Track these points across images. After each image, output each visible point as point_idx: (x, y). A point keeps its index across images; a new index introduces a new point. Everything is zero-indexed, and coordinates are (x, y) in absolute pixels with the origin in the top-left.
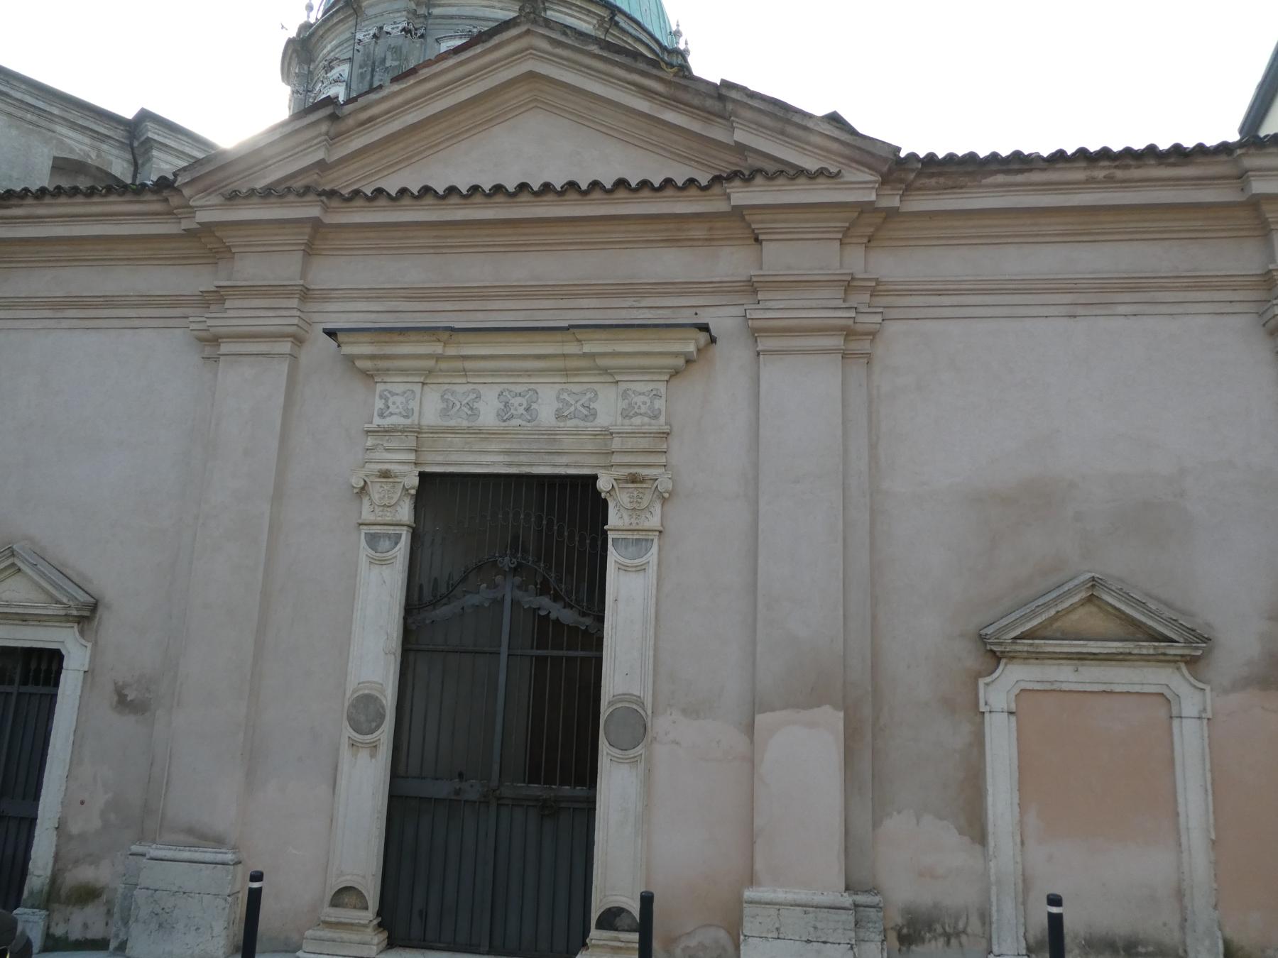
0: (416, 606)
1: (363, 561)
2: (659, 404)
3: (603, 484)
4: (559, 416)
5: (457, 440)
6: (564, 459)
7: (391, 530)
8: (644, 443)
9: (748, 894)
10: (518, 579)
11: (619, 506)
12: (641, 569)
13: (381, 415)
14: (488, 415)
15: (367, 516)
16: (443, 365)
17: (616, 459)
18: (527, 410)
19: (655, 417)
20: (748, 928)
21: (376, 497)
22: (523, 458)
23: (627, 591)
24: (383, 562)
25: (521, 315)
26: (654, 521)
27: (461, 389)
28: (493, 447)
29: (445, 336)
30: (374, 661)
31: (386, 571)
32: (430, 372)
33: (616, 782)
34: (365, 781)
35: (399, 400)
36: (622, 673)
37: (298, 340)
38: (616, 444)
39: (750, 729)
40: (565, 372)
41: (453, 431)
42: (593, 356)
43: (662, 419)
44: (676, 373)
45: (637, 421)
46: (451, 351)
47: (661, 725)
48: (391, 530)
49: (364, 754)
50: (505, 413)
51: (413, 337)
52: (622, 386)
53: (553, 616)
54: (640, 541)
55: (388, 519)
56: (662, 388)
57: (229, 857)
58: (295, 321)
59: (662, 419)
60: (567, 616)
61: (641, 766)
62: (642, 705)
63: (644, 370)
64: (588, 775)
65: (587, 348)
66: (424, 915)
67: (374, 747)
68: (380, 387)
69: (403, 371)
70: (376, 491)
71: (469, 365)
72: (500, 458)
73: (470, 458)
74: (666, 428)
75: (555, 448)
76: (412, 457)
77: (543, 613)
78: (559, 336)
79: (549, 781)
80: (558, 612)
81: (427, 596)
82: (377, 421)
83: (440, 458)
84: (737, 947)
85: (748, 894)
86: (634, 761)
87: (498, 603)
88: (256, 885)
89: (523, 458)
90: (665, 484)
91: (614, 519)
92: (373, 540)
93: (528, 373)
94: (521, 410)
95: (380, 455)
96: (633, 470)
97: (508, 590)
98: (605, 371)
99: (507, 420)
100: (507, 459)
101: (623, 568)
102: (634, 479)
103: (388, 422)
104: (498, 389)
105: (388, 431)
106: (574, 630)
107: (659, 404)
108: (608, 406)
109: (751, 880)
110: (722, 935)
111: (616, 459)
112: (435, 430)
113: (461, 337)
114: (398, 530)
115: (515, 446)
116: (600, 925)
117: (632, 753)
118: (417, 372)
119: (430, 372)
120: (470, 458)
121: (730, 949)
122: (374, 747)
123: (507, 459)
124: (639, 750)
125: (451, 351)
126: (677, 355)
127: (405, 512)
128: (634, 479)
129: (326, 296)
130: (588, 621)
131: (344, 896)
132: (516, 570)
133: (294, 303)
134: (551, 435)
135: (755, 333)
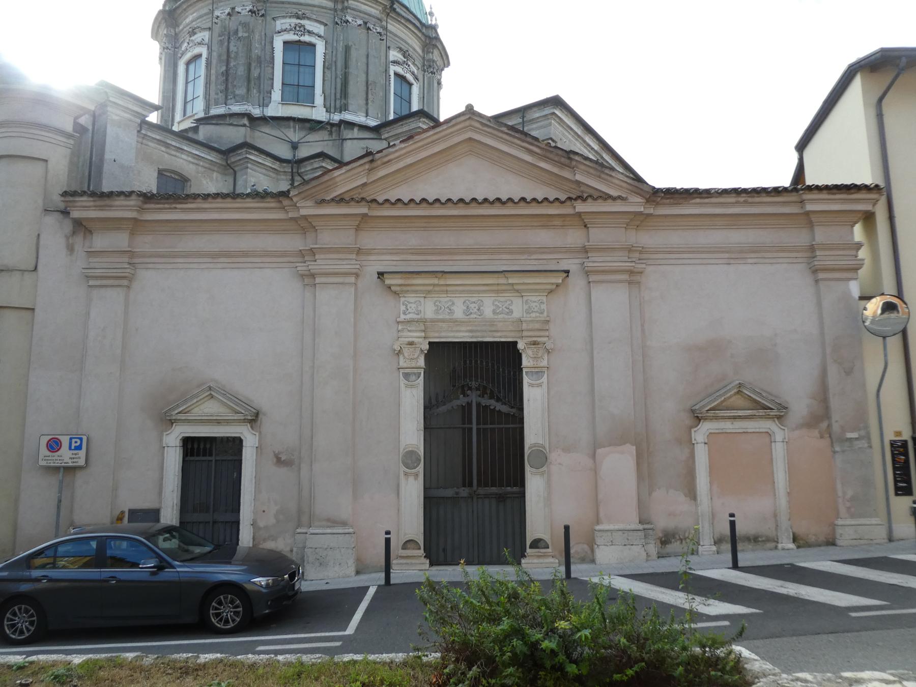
0: (428, 407)
1: (402, 385)
2: (544, 307)
3: (520, 346)
4: (494, 312)
5: (444, 325)
6: (499, 334)
7: (415, 371)
8: (537, 326)
9: (597, 528)
10: (478, 392)
11: (528, 356)
12: (540, 385)
13: (404, 313)
14: (459, 312)
15: (402, 364)
16: (437, 289)
17: (525, 333)
18: (478, 310)
19: (542, 313)
20: (599, 541)
21: (406, 354)
22: (479, 334)
23: (534, 396)
24: (412, 386)
25: (472, 263)
26: (544, 363)
27: (444, 300)
28: (463, 329)
29: (440, 275)
30: (411, 433)
31: (414, 391)
32: (429, 292)
33: (534, 484)
34: (413, 491)
35: (413, 306)
36: (534, 433)
37: (357, 275)
38: (524, 326)
39: (593, 456)
40: (497, 292)
41: (443, 321)
42: (513, 284)
43: (545, 314)
44: (551, 292)
45: (533, 315)
46: (442, 282)
47: (553, 456)
48: (415, 371)
49: (411, 479)
50: (467, 312)
51: (423, 275)
52: (525, 298)
53: (497, 409)
54: (538, 372)
55: (413, 365)
56: (544, 299)
57: (351, 530)
58: (358, 266)
59: (545, 314)
60: (504, 409)
61: (546, 476)
62: (544, 448)
63: (536, 291)
64: (521, 482)
65: (510, 281)
66: (444, 550)
67: (416, 475)
68: (402, 299)
69: (416, 292)
70: (406, 352)
71: (449, 288)
72: (467, 334)
73: (452, 334)
74: (548, 319)
75: (493, 329)
76: (423, 334)
77: (492, 407)
78: (496, 275)
79: (501, 485)
80: (499, 407)
81: (434, 402)
82: (402, 317)
83: (437, 335)
84: (593, 551)
85: (597, 528)
86: (542, 474)
87: (469, 405)
88: (388, 536)
89: (479, 334)
90: (549, 345)
91: (525, 362)
92: (407, 376)
93: (479, 292)
94: (475, 310)
95: (406, 334)
96: (535, 339)
97: (474, 397)
98: (517, 291)
99: (473, 315)
100: (471, 334)
101: (531, 385)
102: (535, 343)
103: (409, 317)
104: (462, 300)
105: (409, 322)
106: (507, 415)
107: (544, 307)
108: (518, 308)
109: (598, 522)
110: (585, 546)
111: (525, 333)
112: (433, 321)
113: (448, 276)
114: (419, 371)
115: (474, 328)
116: (531, 547)
117: (541, 470)
118: (421, 292)
119: (429, 292)
120: (452, 334)
121: (589, 552)
122: (416, 475)
123: (471, 334)
124: (545, 468)
125: (442, 282)
126: (553, 284)
127: (421, 362)
128: (535, 343)
129: (369, 252)
130: (514, 410)
131: (409, 544)
132: (477, 389)
133: (354, 256)
134: (492, 323)
135: (587, 273)
